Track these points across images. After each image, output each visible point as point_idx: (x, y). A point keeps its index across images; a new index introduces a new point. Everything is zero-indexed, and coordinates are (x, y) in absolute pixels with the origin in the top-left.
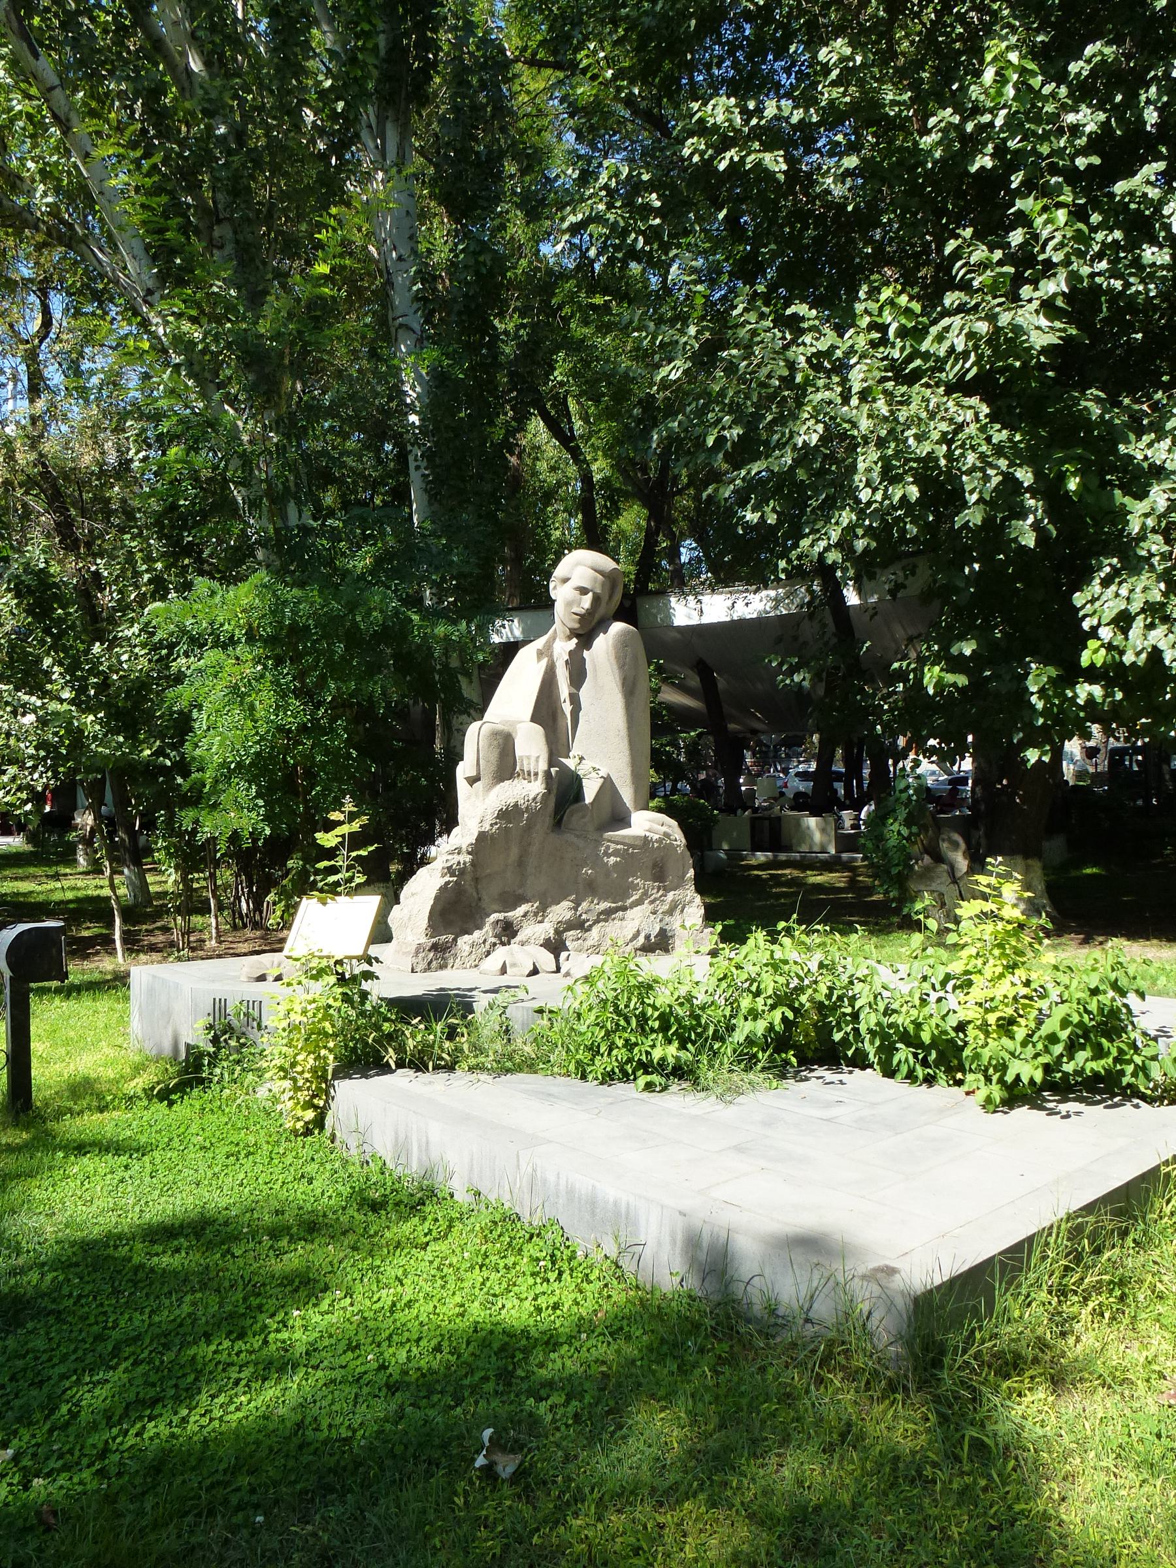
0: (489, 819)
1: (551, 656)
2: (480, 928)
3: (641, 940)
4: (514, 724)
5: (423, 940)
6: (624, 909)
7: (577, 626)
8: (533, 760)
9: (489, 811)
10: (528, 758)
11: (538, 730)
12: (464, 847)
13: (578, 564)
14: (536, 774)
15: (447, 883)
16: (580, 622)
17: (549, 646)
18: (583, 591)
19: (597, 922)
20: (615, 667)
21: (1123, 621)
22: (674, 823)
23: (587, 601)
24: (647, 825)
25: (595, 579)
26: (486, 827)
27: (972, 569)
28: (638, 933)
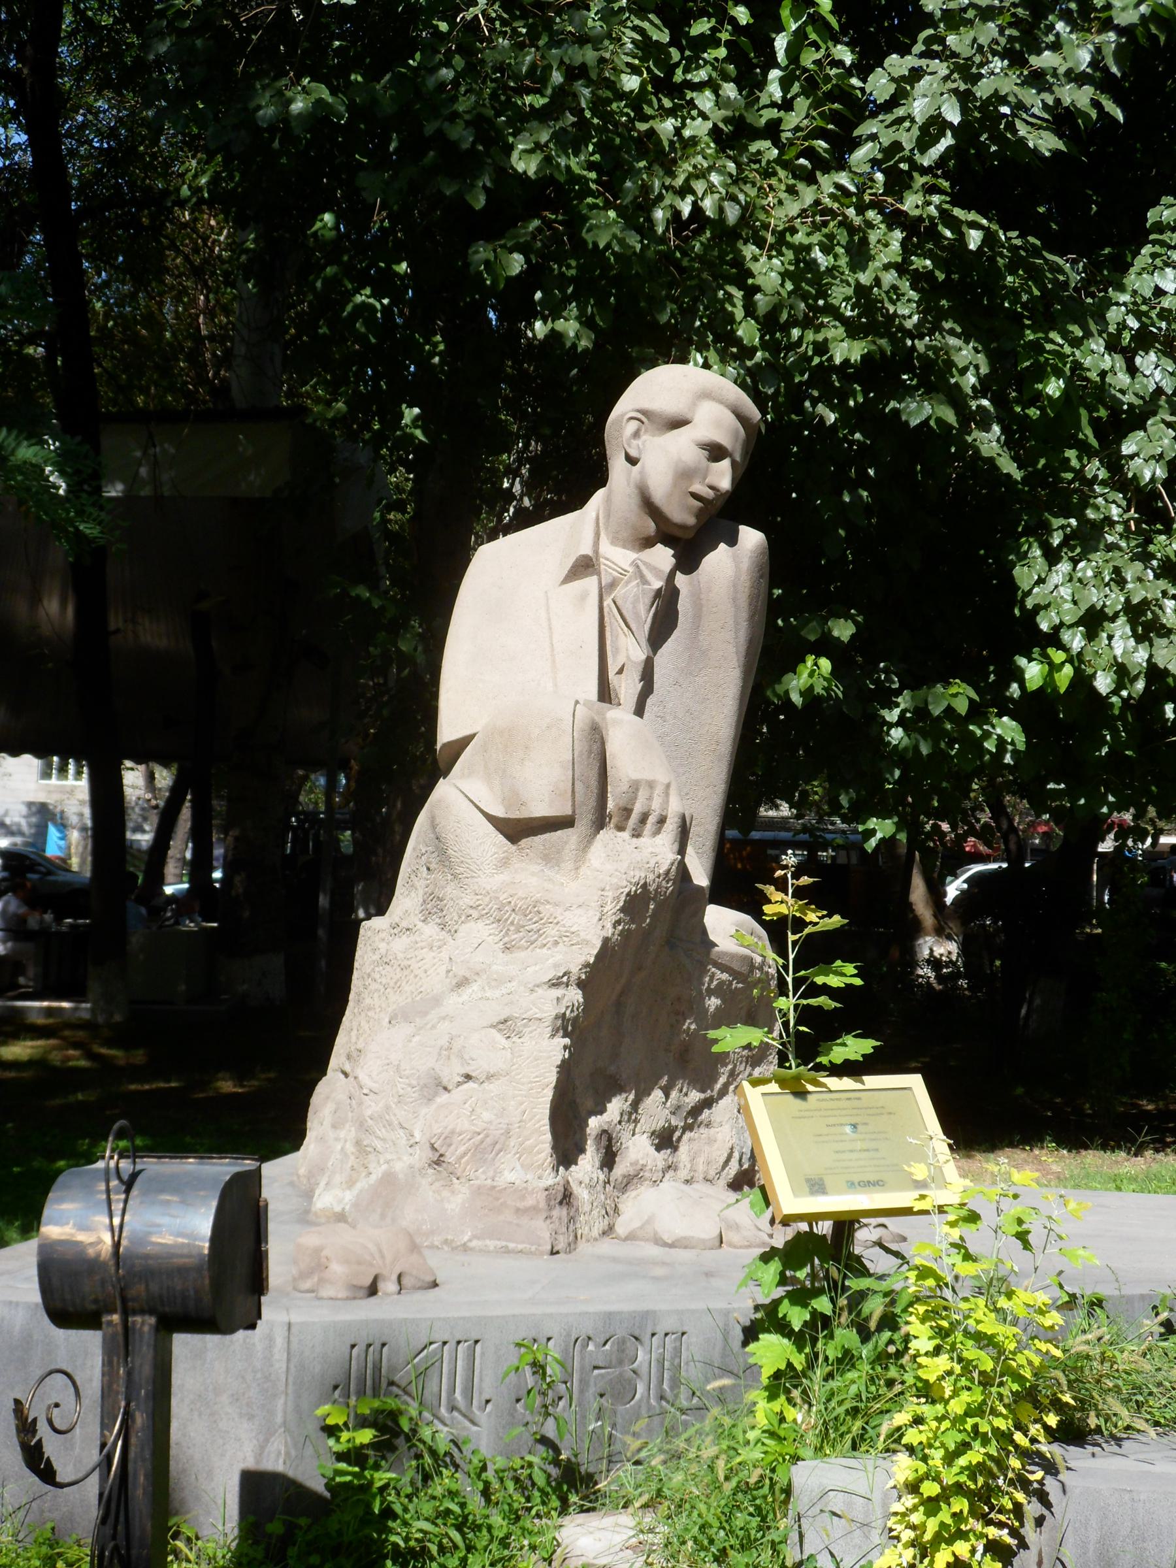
0: (612, 909)
2: (583, 1150)
5: (550, 1179)
7: (691, 520)
8: (659, 790)
9: (610, 894)
10: (651, 785)
12: (575, 969)
13: (706, 395)
14: (662, 821)
16: (699, 514)
18: (716, 452)
20: (744, 615)
21: (1093, 621)
23: (722, 476)
25: (737, 432)
26: (609, 931)
27: (857, 498)
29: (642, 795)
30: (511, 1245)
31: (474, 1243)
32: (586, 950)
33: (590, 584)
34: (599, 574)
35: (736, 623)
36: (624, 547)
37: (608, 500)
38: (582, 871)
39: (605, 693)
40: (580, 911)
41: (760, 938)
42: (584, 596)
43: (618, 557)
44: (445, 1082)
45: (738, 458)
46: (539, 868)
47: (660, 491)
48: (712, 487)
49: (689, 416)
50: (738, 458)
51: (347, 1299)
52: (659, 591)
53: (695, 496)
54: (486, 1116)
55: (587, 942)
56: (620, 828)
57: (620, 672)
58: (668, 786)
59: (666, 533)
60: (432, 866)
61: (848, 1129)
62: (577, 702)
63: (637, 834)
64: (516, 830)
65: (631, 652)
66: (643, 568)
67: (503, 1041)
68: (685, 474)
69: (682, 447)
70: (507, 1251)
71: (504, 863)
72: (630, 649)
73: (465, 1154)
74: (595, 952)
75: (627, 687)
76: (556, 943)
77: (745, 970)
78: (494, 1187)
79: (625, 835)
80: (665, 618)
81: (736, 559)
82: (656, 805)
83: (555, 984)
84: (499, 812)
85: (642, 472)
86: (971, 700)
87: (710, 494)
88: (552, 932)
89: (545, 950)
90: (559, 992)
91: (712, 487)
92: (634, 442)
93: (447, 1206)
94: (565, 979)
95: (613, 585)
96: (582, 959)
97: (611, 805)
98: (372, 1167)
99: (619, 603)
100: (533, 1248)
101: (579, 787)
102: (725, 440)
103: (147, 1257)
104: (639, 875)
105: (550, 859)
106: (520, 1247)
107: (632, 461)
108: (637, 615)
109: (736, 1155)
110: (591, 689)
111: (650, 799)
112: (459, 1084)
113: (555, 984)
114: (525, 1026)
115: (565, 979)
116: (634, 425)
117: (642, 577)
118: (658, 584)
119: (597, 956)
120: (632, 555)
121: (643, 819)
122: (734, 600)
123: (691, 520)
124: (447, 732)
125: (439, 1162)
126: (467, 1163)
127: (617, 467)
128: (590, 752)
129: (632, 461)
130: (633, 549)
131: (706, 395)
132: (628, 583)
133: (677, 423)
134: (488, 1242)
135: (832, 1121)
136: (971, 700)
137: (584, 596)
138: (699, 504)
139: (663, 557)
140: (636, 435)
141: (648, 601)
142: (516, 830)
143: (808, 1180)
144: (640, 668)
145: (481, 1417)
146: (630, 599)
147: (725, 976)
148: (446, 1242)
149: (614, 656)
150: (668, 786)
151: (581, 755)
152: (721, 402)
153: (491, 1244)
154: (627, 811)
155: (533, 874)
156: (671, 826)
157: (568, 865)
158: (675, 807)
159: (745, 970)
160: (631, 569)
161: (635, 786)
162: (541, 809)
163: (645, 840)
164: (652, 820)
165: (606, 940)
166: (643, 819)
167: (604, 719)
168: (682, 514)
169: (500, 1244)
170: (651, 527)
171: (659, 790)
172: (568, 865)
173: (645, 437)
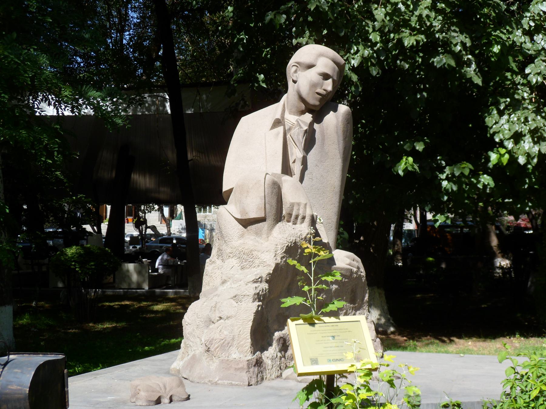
0: (280, 252)
2: (271, 345)
5: (250, 357)
7: (317, 103)
8: (302, 206)
9: (279, 247)
10: (299, 204)
12: (264, 276)
13: (321, 55)
14: (304, 218)
15: (259, 306)
16: (320, 101)
18: (326, 76)
20: (341, 138)
21: (517, 137)
22: (359, 260)
23: (329, 85)
24: (348, 261)
26: (279, 261)
27: (422, 96)
30: (233, 382)
31: (219, 382)
32: (269, 268)
33: (280, 129)
34: (284, 125)
35: (339, 142)
36: (294, 115)
37: (287, 97)
38: (270, 238)
39: (286, 170)
40: (267, 253)
41: (357, 262)
42: (278, 134)
43: (291, 118)
44: (213, 320)
45: (335, 78)
46: (254, 237)
47: (305, 92)
48: (325, 90)
49: (314, 63)
50: (335, 78)
51: (147, 405)
52: (306, 130)
53: (318, 93)
54: (226, 333)
55: (269, 265)
56: (289, 221)
57: (294, 162)
58: (306, 204)
59: (309, 109)
60: (220, 238)
61: (331, 338)
62: (267, 174)
63: (295, 224)
64: (246, 223)
65: (297, 154)
66: (300, 122)
67: (236, 304)
68: (314, 85)
69: (312, 75)
70: (232, 385)
71: (242, 236)
72: (296, 153)
73: (217, 347)
74: (273, 269)
75: (297, 168)
76: (259, 266)
77: (348, 274)
78: (228, 360)
79: (291, 224)
80: (310, 141)
81: (337, 117)
82: (301, 212)
83: (255, 281)
84: (239, 217)
85: (298, 86)
86: (470, 170)
87: (324, 92)
88: (257, 262)
89: (255, 269)
90: (256, 285)
91: (325, 90)
92: (295, 75)
93: (211, 367)
94: (260, 280)
95: (290, 129)
96: (267, 272)
97: (284, 213)
98: (189, 352)
99: (292, 136)
100: (241, 383)
101: (267, 206)
102: (329, 72)
103: (6, 394)
104: (293, 239)
105: (258, 233)
106: (237, 383)
107: (295, 82)
108: (299, 140)
110: (278, 168)
111: (299, 209)
112: (218, 321)
113: (255, 281)
114: (243, 298)
115: (260, 280)
116: (295, 68)
117: (300, 125)
118: (305, 128)
119: (273, 270)
120: (297, 117)
121: (297, 217)
122: (337, 133)
123: (317, 103)
124: (225, 188)
125: (208, 350)
126: (218, 351)
127: (290, 84)
128: (272, 193)
129: (295, 82)
130: (297, 115)
131: (321, 55)
132: (295, 128)
133: (310, 66)
134: (224, 381)
135: (324, 335)
136: (470, 170)
137: (278, 134)
138: (320, 97)
139: (308, 117)
140: (296, 72)
141: (302, 134)
142: (246, 223)
143: (311, 359)
144: (301, 160)
146: (296, 134)
148: (210, 381)
149: (291, 156)
150: (306, 204)
151: (268, 194)
152: (327, 57)
153: (226, 382)
154: (290, 215)
155: (251, 240)
156: (308, 220)
157: (264, 236)
158: (308, 213)
159: (348, 274)
160: (296, 123)
161: (292, 205)
162: (253, 215)
163: (298, 225)
164: (300, 218)
165: (277, 265)
166: (297, 217)
167: (281, 180)
168: (313, 101)
169: (229, 382)
170: (303, 107)
171: (302, 206)
172: (264, 236)
173: (299, 72)
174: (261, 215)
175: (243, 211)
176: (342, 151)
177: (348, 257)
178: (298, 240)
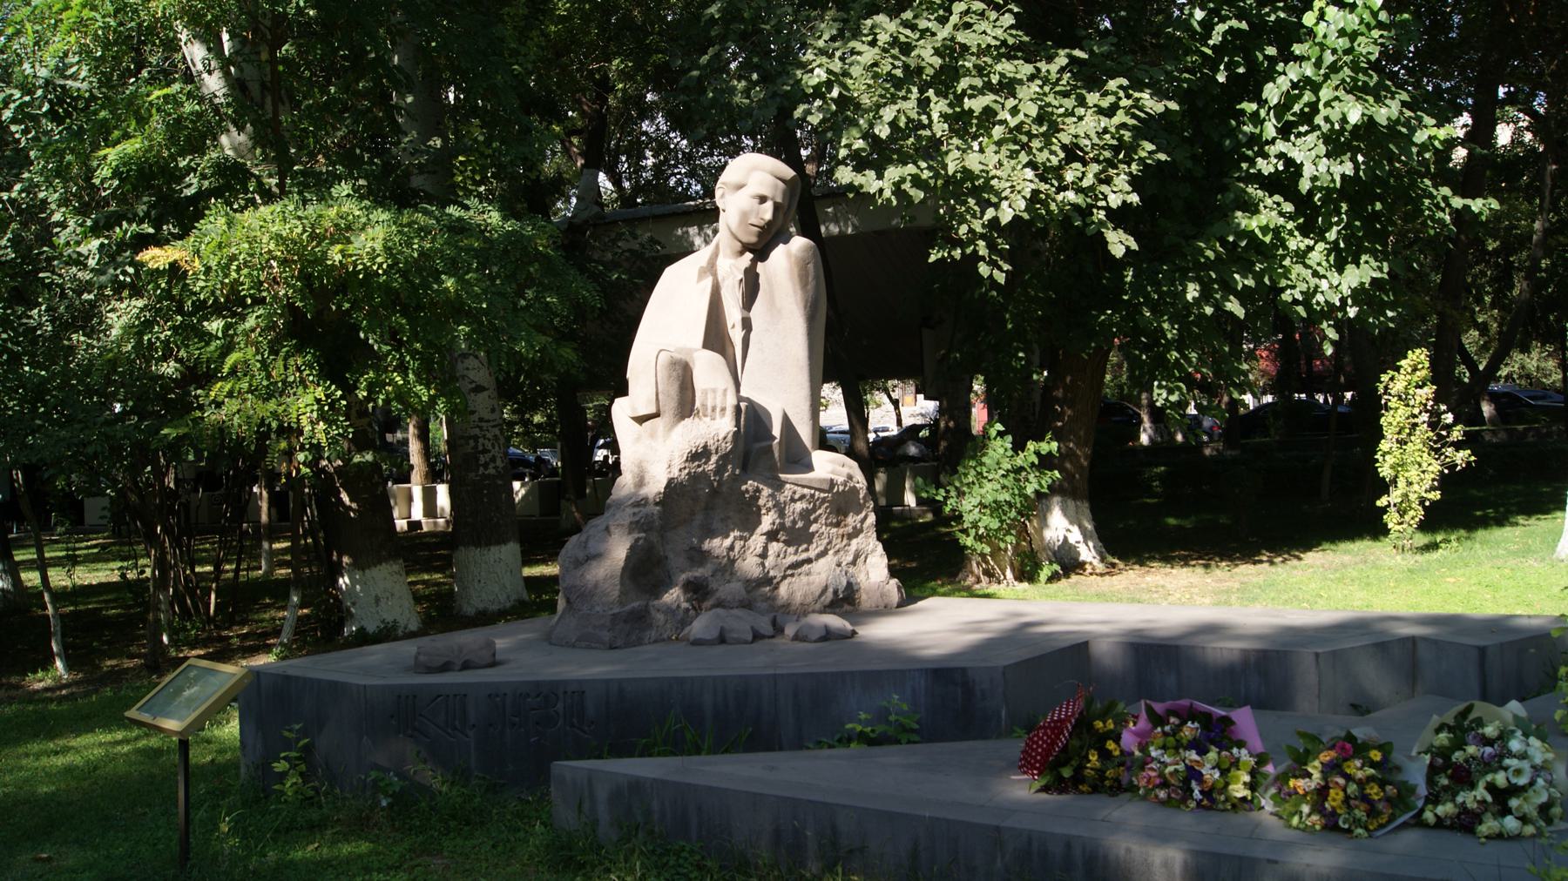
0: (678, 462)
1: (715, 275)
3: (829, 595)
4: (691, 351)
6: (809, 561)
7: (753, 239)
9: (677, 454)
10: (714, 391)
11: (716, 357)
13: (755, 168)
14: (723, 410)
15: (637, 540)
17: (711, 268)
18: (763, 199)
19: (784, 577)
20: (798, 287)
22: (855, 464)
23: (767, 212)
24: (830, 467)
25: (776, 186)
26: (675, 473)
28: (826, 588)
29: (710, 396)
47: (734, 227)
59: (746, 248)
64: (641, 420)
68: (744, 215)
71: (638, 439)
77: (826, 487)
81: (789, 255)
87: (762, 223)
109: (831, 590)
120: (732, 261)
121: (714, 409)
133: (740, 187)
142: (641, 420)
145: (471, 733)
147: (806, 491)
154: (704, 405)
159: (826, 487)
161: (705, 392)
165: (670, 481)
166: (714, 409)
174: (653, 410)
175: (634, 409)
176: (801, 305)
177: (832, 462)
178: (710, 442)
